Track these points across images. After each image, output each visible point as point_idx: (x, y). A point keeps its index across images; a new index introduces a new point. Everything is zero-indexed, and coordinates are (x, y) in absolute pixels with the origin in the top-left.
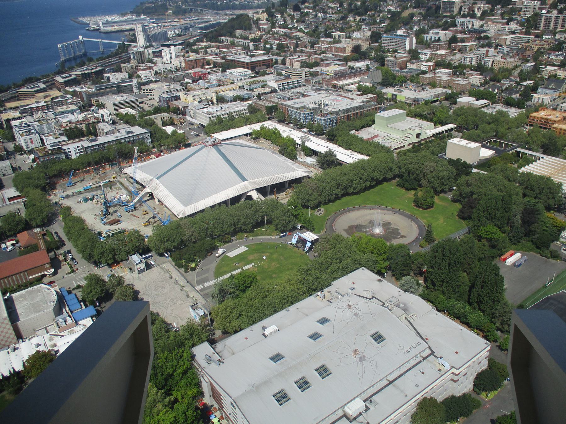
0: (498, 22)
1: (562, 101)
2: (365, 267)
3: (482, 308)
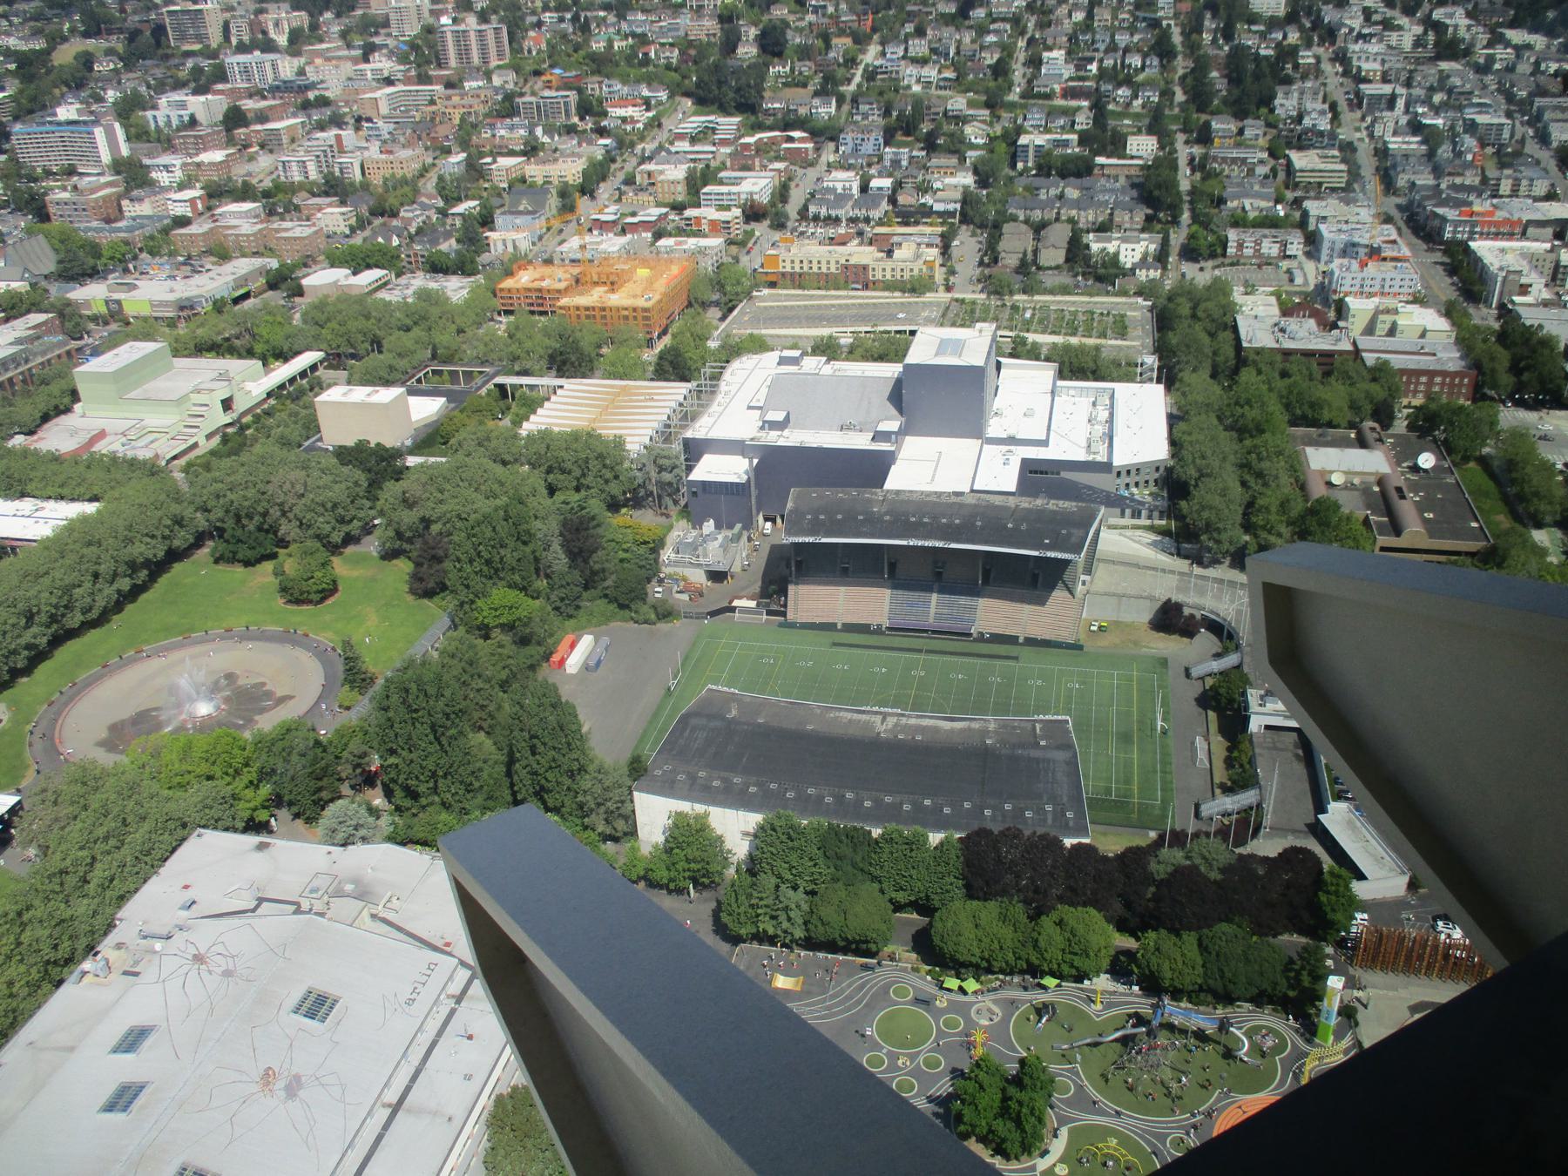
0: (339, 58)
1: (558, 239)
2: (204, 827)
3: (551, 803)
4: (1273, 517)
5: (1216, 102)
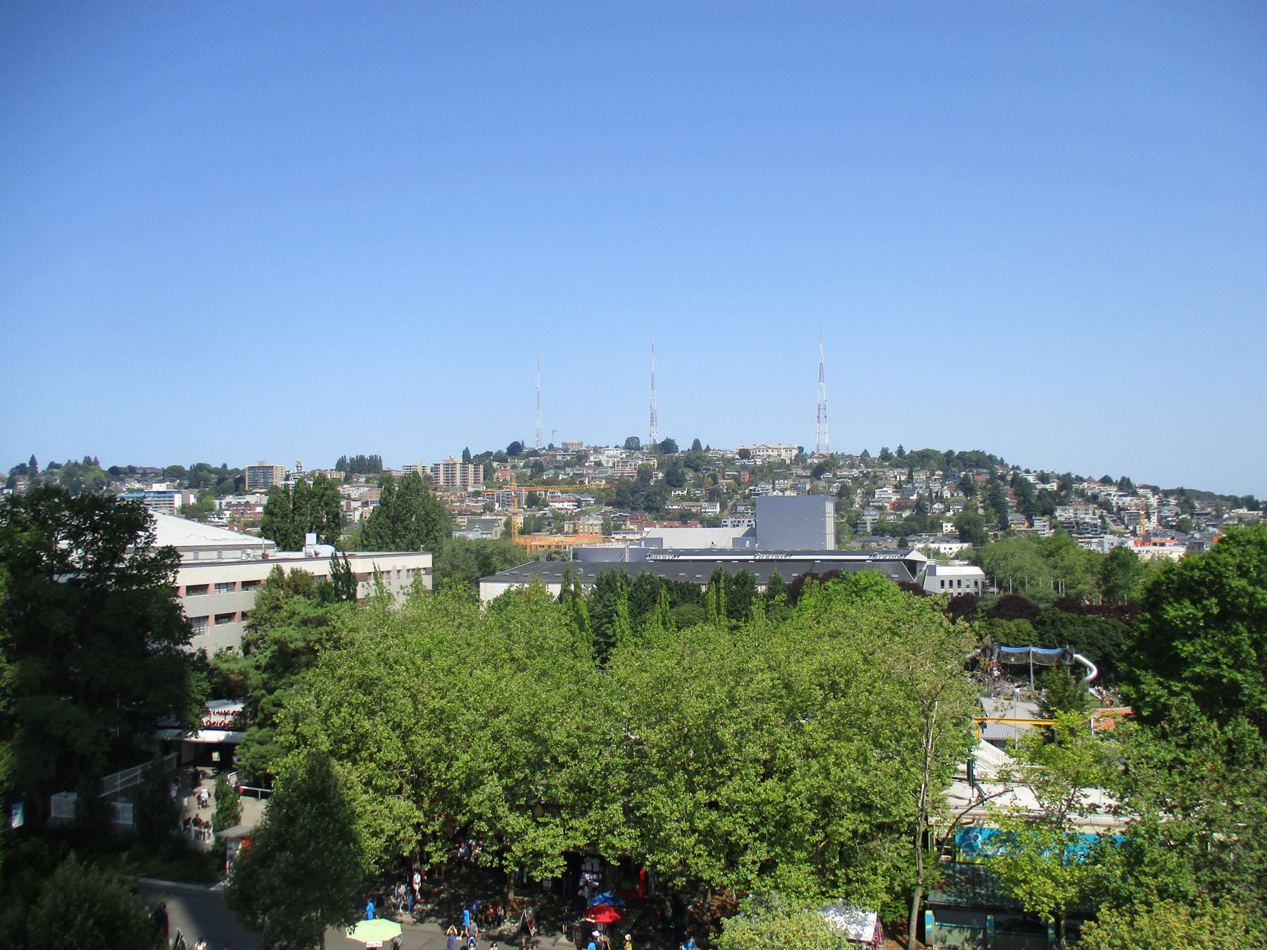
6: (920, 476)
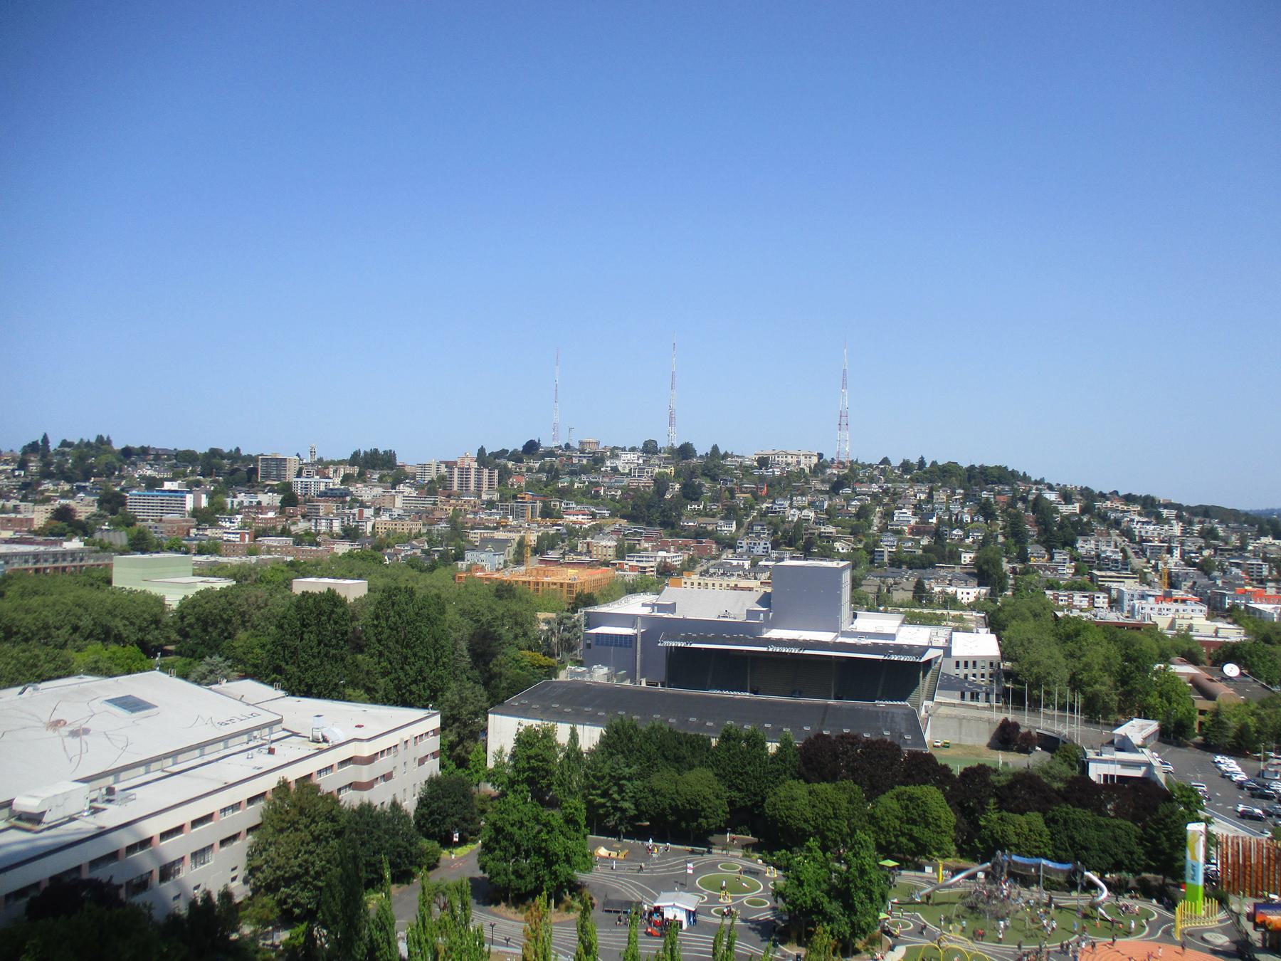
4: (1096, 673)
5: (1030, 540)
6: (941, 496)
